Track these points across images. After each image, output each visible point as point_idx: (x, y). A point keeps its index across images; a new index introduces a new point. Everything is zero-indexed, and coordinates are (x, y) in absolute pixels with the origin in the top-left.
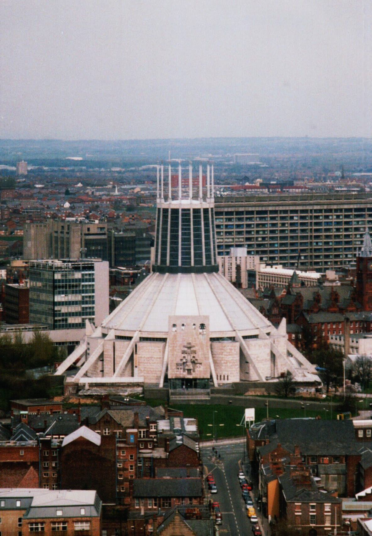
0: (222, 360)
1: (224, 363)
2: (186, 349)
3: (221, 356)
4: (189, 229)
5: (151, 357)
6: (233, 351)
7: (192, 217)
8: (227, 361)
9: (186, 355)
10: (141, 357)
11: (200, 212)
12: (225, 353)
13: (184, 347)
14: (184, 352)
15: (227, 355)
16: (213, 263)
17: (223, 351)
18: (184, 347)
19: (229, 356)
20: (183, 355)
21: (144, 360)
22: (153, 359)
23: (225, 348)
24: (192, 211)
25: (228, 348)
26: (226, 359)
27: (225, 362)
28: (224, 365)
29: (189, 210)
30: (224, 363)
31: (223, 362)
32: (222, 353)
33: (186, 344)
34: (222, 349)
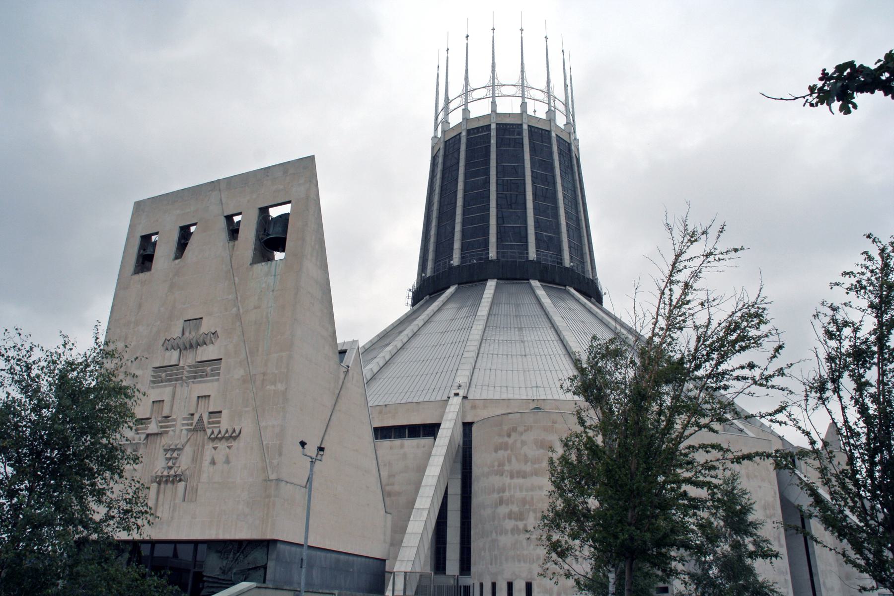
0: (501, 502)
1: (510, 516)
2: (173, 357)
3: (496, 481)
4: (487, 172)
7: (493, 141)
8: (524, 502)
11: (520, 133)
12: (516, 466)
15: (524, 477)
16: (567, 263)
17: (501, 453)
23: (513, 435)
24: (493, 126)
25: (530, 437)
26: (519, 495)
27: (515, 508)
28: (509, 524)
30: (510, 516)
31: (503, 510)
32: (501, 464)
33: (176, 332)
34: (504, 447)
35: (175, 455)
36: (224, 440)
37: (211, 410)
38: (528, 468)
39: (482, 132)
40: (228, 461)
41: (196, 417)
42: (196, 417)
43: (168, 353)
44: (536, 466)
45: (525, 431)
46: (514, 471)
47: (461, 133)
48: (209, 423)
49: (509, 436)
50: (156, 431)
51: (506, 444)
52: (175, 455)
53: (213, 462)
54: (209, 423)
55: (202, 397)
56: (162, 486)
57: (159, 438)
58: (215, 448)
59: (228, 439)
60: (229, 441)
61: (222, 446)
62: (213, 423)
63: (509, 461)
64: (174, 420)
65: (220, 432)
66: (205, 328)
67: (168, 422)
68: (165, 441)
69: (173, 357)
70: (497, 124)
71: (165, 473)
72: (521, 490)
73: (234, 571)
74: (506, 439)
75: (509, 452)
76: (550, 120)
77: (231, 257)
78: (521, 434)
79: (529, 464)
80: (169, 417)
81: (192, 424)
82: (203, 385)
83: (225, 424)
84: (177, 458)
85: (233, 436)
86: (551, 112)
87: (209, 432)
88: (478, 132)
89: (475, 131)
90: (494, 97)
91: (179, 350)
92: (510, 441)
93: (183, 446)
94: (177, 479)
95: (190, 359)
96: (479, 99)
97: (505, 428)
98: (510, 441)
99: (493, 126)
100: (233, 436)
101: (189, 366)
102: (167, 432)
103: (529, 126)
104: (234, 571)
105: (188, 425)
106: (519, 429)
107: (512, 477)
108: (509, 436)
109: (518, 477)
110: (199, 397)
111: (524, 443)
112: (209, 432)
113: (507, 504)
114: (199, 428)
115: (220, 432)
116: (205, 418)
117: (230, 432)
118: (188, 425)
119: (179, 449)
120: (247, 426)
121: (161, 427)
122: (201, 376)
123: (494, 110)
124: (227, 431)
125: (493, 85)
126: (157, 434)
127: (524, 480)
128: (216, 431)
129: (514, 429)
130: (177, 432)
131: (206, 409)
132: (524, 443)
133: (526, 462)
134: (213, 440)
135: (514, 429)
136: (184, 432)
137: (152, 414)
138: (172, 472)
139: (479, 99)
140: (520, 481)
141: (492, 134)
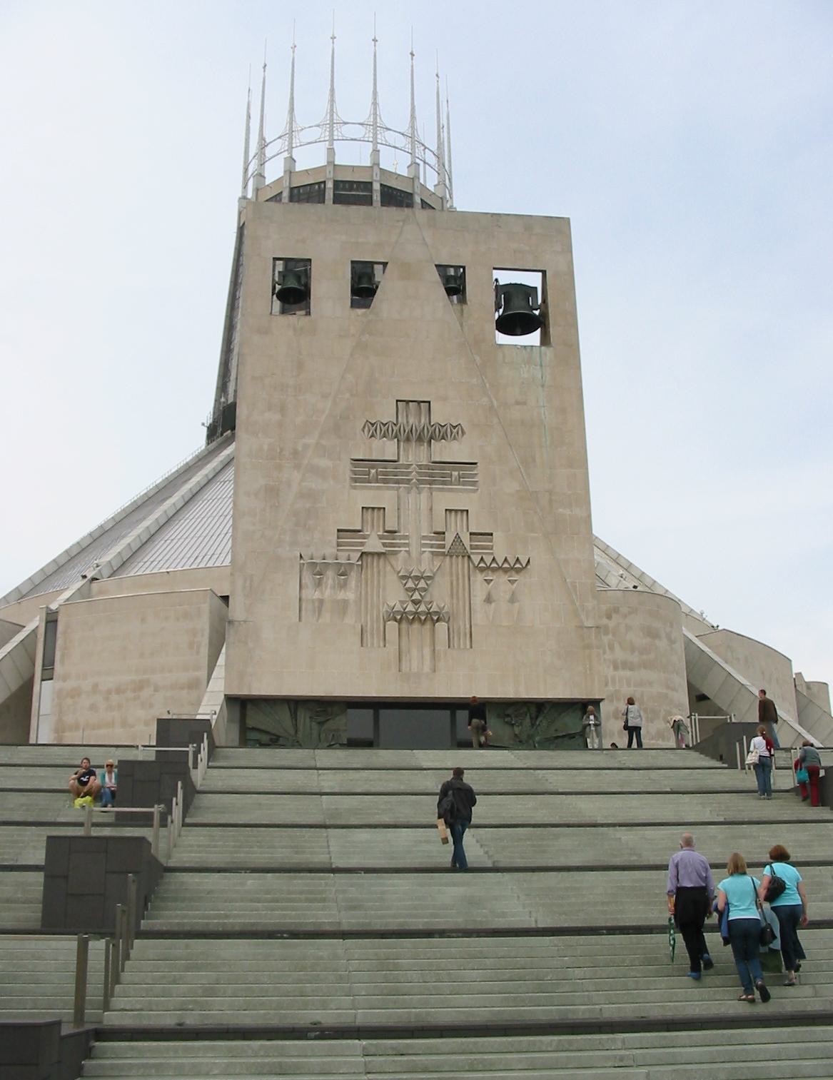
2: (388, 449)
5: (139, 686)
6: (662, 644)
9: (385, 497)
10: (75, 693)
13: (375, 429)
14: (367, 471)
15: (631, 669)
18: (375, 429)
19: (644, 674)
20: (368, 496)
21: (93, 707)
22: (146, 693)
23: (614, 616)
24: (376, 186)
29: (368, 185)
33: (386, 413)
35: (422, 584)
36: (501, 572)
37: (470, 531)
38: (635, 658)
39: (357, 190)
40: (513, 600)
41: (450, 538)
42: (450, 538)
43: (377, 443)
44: (645, 657)
45: (630, 613)
46: (619, 661)
47: (324, 182)
48: (472, 547)
49: (609, 617)
50: (383, 550)
51: (606, 627)
52: (422, 584)
53: (489, 600)
54: (472, 547)
55: (451, 511)
56: (404, 625)
57: (382, 561)
58: (488, 582)
59: (506, 571)
60: (509, 574)
61: (501, 579)
62: (477, 547)
63: (611, 648)
64: (406, 537)
65: (494, 559)
66: (438, 416)
67: (394, 539)
68: (399, 562)
69: (388, 449)
70: (381, 185)
71: (410, 608)
72: (629, 685)
73: (537, 739)
74: (605, 621)
75: (610, 636)
76: (441, 198)
77: (461, 325)
78: (626, 616)
79: (637, 653)
80: (395, 532)
81: (443, 546)
82: (447, 494)
83: (501, 549)
84: (425, 590)
85: (516, 568)
86: (441, 183)
87: (476, 559)
88: (351, 189)
89: (347, 186)
90: (375, 142)
91: (396, 440)
92: (611, 624)
93: (434, 575)
94: (433, 618)
95: (415, 456)
96: (352, 140)
97: (604, 607)
98: (611, 624)
99: (376, 186)
100: (516, 568)
101: (420, 467)
102: (395, 553)
103: (422, 200)
104: (537, 739)
105: (432, 546)
106: (624, 610)
107: (616, 668)
108: (609, 617)
109: (623, 669)
110: (446, 510)
111: (628, 628)
112: (476, 559)
113: (612, 701)
114: (458, 551)
115: (494, 559)
116: (466, 539)
117: (512, 562)
118: (432, 546)
119: (429, 578)
120: (538, 555)
121: (384, 545)
122: (444, 483)
123: (376, 164)
124: (506, 560)
125: (375, 125)
126: (379, 554)
127: (631, 672)
128: (488, 560)
129: (616, 610)
130: (414, 554)
131: (465, 530)
132: (628, 628)
133: (633, 651)
134: (482, 570)
135: (616, 610)
136: (427, 555)
137: (362, 526)
138: (422, 608)
139: (352, 140)
140: (628, 673)
141: (375, 198)
